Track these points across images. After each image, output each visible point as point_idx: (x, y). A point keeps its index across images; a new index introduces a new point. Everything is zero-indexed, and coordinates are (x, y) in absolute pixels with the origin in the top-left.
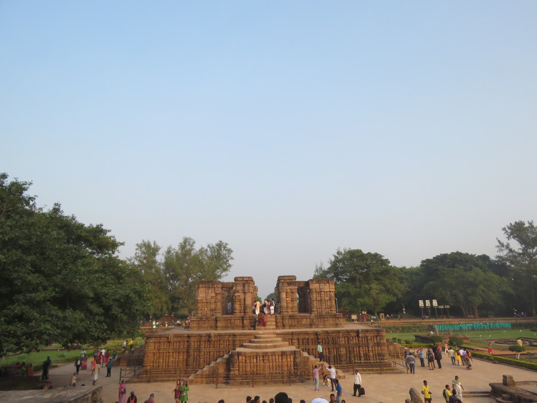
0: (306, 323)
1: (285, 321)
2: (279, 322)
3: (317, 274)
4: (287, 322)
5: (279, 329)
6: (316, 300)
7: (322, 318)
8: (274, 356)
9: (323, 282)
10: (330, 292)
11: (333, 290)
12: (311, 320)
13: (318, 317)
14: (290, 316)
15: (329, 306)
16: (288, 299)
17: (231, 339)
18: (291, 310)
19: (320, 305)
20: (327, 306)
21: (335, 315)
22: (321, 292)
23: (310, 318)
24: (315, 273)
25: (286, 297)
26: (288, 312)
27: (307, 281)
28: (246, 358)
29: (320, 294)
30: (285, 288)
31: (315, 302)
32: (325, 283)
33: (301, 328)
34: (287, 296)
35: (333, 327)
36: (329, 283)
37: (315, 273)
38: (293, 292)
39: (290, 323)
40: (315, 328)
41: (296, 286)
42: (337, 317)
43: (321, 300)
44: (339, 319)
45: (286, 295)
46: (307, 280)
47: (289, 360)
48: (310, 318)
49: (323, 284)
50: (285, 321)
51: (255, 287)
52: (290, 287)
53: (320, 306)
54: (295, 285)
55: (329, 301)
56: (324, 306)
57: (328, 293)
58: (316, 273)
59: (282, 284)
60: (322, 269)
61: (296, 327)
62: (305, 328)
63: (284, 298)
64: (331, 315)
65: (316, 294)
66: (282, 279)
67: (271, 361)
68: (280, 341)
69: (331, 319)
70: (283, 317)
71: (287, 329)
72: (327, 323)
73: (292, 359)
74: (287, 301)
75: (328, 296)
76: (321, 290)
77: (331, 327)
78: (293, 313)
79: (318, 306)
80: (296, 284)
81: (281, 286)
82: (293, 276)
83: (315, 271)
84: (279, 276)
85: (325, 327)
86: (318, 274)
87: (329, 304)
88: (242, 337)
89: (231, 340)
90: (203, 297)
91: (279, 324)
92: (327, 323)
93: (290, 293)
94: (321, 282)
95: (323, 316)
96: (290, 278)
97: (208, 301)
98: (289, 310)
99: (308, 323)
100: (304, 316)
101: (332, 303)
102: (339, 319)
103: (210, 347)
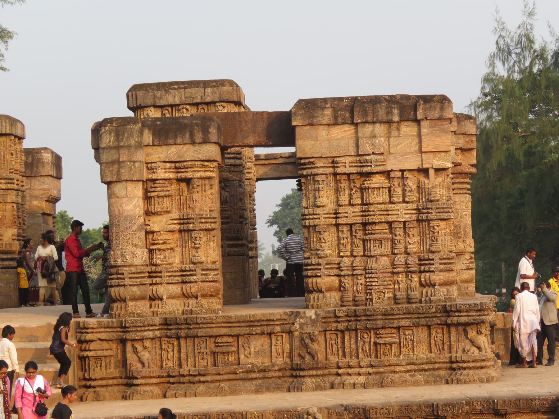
0: (267, 362)
1: (135, 352)
2: (96, 358)
3: (501, 71)
4: (146, 356)
5: (98, 398)
6: (337, 225)
7: (367, 329)
9: (382, 114)
10: (425, 172)
11: (438, 162)
12: (296, 343)
13: (341, 326)
14: (166, 323)
15: (413, 260)
16: (156, 224)
18: (176, 289)
19: (359, 251)
20: (400, 259)
21: (447, 311)
22: (368, 175)
23: (290, 332)
24: (492, 65)
25: (148, 213)
27: (288, 110)
29: (362, 190)
30: (140, 156)
31: (330, 236)
32: (389, 122)
33: (233, 392)
34: (156, 208)
35: (427, 382)
36: (418, 122)
37: (492, 65)
38: (188, 181)
39: (170, 365)
40: (318, 388)
41: (206, 141)
42: (458, 325)
43: (365, 225)
44: (472, 333)
45: (147, 198)
46: (287, 106)
48: (290, 332)
49: (380, 129)
50: (135, 352)
51: (29, 152)
53: (358, 261)
54: (199, 137)
55: (412, 232)
56: (385, 261)
57: (411, 183)
58: (498, 64)
59: (118, 135)
60: (531, 42)
61: (202, 387)
62: (258, 390)
63: (130, 219)
64: (424, 314)
65: (337, 190)
66: (149, 101)
69: (422, 333)
70: (124, 328)
71: (144, 396)
72: (393, 359)
75: (413, 196)
76: (362, 163)
77: (417, 384)
78: (192, 302)
79: (346, 261)
80: (205, 131)
81: (109, 148)
82: (219, 83)
83: (493, 57)
84: (136, 88)
85: (381, 385)
86: (511, 70)
87: (413, 248)
91: (97, 372)
92: (393, 359)
93: (173, 188)
94: (365, 113)
95: (369, 317)
96: (197, 95)
98: (161, 290)
99: (280, 361)
100: (251, 323)
101: (434, 239)
102: (472, 333)
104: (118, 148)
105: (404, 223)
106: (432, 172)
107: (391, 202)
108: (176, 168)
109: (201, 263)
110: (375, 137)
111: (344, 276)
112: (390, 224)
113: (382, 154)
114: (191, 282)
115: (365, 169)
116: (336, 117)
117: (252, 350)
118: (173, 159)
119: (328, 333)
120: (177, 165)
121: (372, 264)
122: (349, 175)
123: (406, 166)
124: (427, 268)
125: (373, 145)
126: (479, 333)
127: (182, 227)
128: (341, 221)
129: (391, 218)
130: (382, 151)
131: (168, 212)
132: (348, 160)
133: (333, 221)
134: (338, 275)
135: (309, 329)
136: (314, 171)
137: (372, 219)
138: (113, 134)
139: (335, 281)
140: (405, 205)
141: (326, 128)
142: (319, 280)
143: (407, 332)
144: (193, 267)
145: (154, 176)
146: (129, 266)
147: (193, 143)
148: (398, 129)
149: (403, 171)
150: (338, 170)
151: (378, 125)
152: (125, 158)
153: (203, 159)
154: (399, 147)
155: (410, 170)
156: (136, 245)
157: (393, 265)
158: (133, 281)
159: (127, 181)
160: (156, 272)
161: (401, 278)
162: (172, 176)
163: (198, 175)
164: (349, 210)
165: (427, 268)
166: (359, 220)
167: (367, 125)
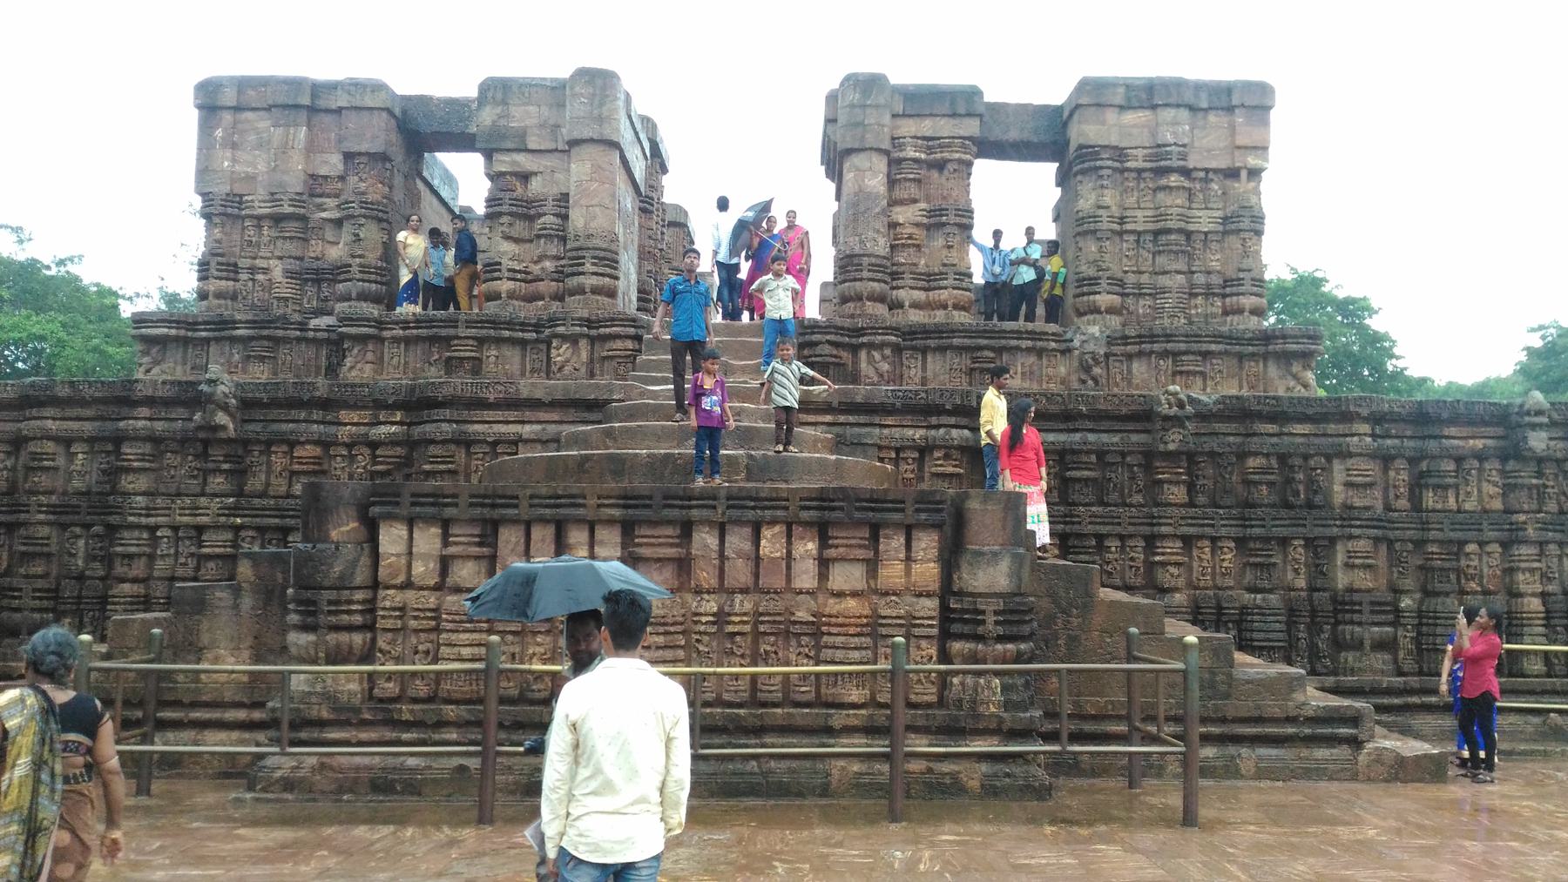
1: (871, 360)
8: (747, 531)
16: (902, 215)
17: (384, 430)
18: (920, 295)
26: (895, 305)
27: (1059, 103)
28: (446, 544)
43: (1157, 233)
44: (1296, 367)
45: (892, 183)
47: (892, 573)
52: (927, 127)
67: (705, 575)
68: (816, 440)
73: (927, 571)
74: (893, 225)
88: (489, 415)
89: (393, 442)
90: (251, 178)
97: (287, 209)
103: (203, 494)
104: (864, 106)
105: (1206, 234)
106: (1244, 174)
107: (1190, 208)
108: (929, 148)
109: (954, 265)
110: (1178, 124)
111: (1127, 295)
112: (1188, 235)
113: (1184, 146)
114: (941, 288)
115: (1163, 163)
116: (1129, 99)
117: (1019, 369)
118: (927, 134)
119: (1111, 358)
120: (930, 143)
121: (1164, 281)
122: (1139, 171)
123: (1213, 165)
124: (1234, 289)
125: (1174, 133)
126: (1307, 367)
127: (932, 220)
128: (1129, 227)
129: (1191, 227)
130: (1186, 141)
131: (915, 201)
132: (1140, 153)
133: (1116, 227)
134: (1123, 295)
135: (1090, 347)
136: (1098, 163)
137: (1170, 225)
138: (858, 89)
139: (1116, 300)
140: (1209, 213)
141: (1117, 110)
142: (1097, 297)
143: (1214, 361)
144: (944, 270)
145: (902, 155)
146: (869, 256)
147: (954, 115)
148: (1205, 118)
149: (1207, 171)
150: (1129, 164)
151: (1182, 109)
152: (873, 121)
153: (966, 135)
154: (1205, 141)
155: (1216, 171)
156: (878, 231)
157: (1192, 286)
158: (874, 275)
159: (871, 149)
160: (897, 273)
161: (1200, 300)
162: (923, 156)
163: (957, 156)
164: (1139, 213)
165: (1234, 289)
166: (1151, 226)
167: (1169, 109)
